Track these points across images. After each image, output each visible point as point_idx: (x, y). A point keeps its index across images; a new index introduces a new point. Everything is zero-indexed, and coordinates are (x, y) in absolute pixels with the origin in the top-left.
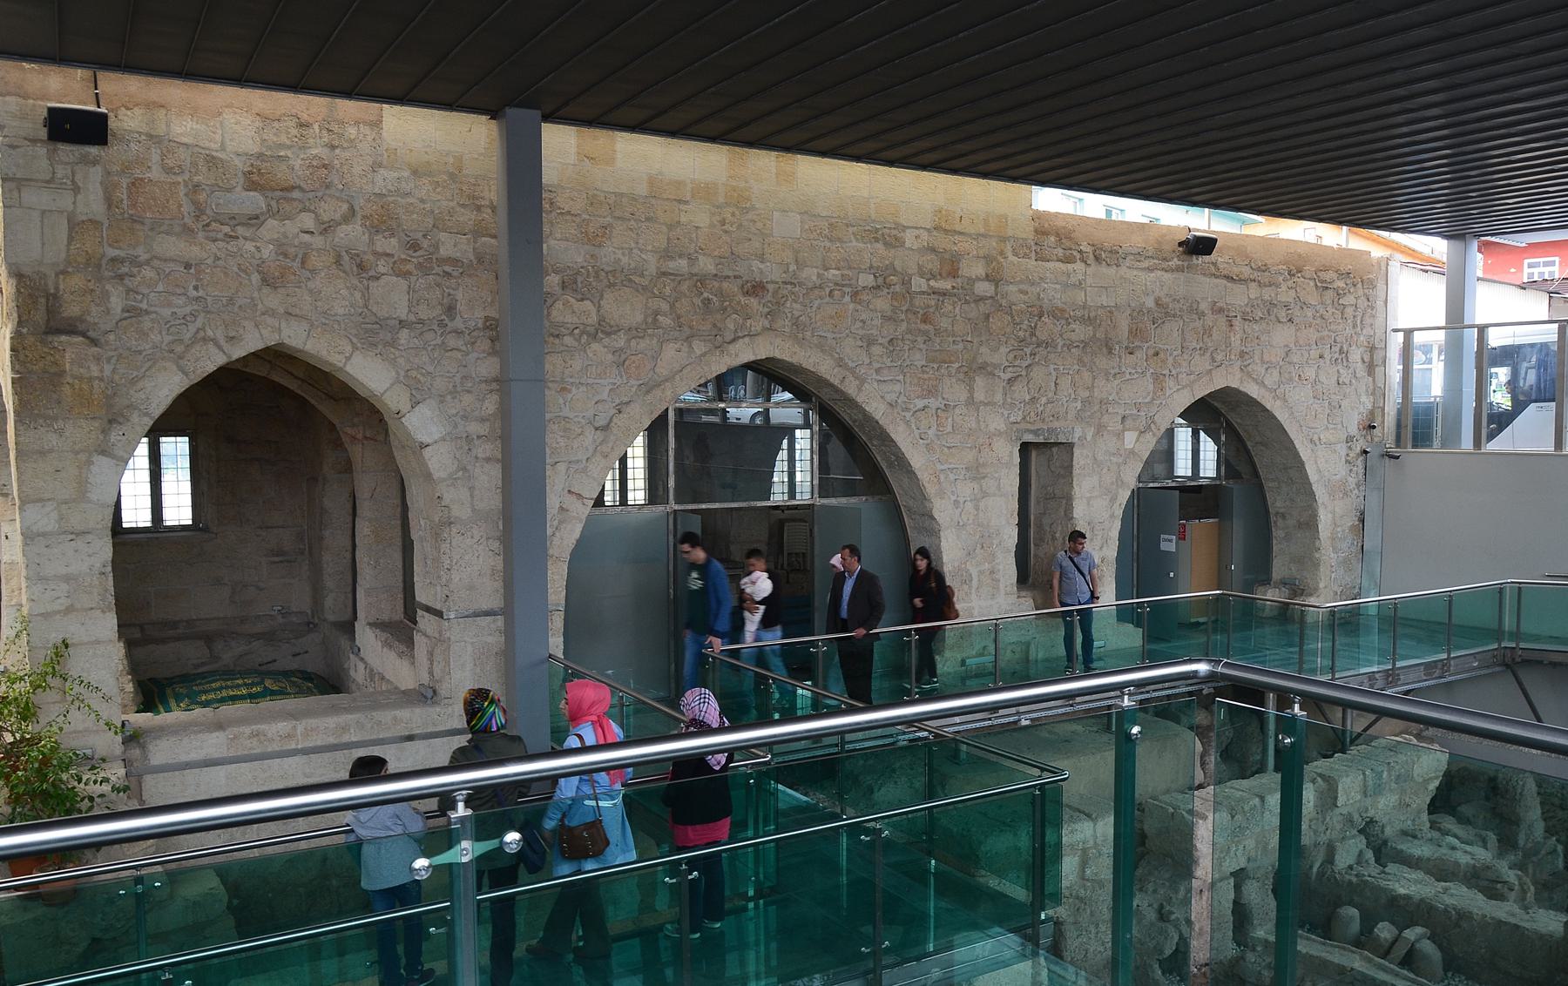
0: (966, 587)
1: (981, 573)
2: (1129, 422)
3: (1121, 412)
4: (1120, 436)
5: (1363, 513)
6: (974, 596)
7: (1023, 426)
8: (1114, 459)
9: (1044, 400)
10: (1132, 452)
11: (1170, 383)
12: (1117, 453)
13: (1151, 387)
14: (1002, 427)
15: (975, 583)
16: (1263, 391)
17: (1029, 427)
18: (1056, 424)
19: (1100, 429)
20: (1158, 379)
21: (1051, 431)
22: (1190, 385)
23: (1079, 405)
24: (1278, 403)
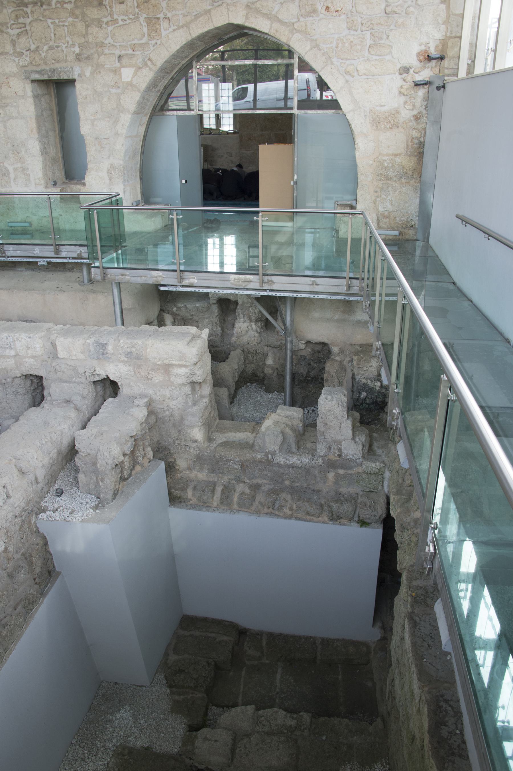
0: (6, 178)
1: (15, 170)
2: (125, 61)
3: (117, 52)
4: (116, 72)
5: (422, 145)
6: (12, 184)
7: (30, 68)
8: (114, 91)
9: (46, 48)
10: (130, 84)
11: (164, 24)
12: (116, 85)
13: (145, 30)
14: (15, 70)
15: (12, 176)
16: (276, 25)
17: (38, 69)
18: (57, 65)
19: (98, 68)
20: (153, 23)
21: (54, 71)
22: (187, 25)
23: (77, 50)
24: (297, 36)
